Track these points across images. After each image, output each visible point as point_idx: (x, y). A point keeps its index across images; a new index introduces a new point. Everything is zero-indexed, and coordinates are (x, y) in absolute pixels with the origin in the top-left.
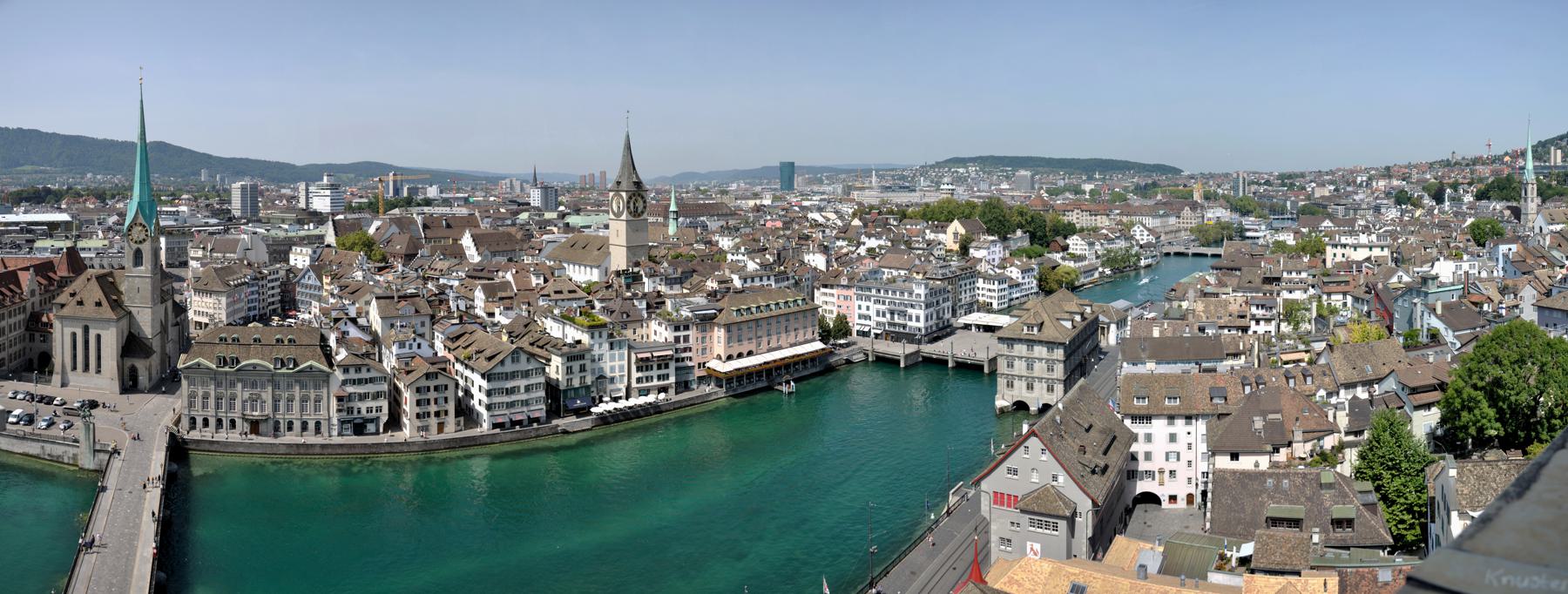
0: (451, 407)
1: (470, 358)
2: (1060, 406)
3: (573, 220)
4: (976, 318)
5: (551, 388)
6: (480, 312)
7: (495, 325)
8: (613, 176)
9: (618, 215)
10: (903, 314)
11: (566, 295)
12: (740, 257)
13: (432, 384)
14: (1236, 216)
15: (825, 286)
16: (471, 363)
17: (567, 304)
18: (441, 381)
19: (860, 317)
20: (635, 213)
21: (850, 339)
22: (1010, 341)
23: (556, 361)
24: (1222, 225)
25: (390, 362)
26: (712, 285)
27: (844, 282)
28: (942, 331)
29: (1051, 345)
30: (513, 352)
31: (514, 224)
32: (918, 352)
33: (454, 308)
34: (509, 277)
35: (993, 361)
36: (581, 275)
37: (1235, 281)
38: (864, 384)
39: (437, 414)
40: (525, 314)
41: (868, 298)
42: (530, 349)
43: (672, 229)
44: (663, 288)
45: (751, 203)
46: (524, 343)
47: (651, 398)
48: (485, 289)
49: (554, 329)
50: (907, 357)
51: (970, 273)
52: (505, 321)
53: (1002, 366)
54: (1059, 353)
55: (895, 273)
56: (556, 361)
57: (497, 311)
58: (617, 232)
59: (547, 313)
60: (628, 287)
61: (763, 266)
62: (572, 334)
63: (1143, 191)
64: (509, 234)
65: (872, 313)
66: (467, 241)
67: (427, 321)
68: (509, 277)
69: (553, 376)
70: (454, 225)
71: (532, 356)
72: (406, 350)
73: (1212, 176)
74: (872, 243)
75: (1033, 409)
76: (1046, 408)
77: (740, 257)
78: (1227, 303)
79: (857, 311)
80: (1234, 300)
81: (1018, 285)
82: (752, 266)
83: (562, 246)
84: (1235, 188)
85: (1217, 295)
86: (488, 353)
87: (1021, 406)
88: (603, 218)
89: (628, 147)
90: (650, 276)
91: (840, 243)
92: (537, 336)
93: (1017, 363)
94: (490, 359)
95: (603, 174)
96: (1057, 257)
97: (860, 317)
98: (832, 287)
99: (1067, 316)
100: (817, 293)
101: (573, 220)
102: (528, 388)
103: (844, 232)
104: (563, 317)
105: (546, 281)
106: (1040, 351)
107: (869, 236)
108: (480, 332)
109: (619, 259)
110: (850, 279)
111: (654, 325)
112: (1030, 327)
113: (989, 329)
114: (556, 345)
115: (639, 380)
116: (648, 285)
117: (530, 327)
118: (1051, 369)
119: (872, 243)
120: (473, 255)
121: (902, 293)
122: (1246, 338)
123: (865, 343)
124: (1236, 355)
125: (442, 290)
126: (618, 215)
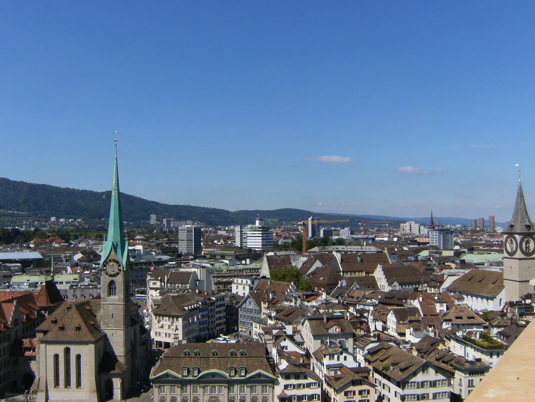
1: (386, 368)
7: (407, 343)
11: (465, 321)
13: (357, 388)
16: (388, 373)
40: (432, 335)
42: (436, 363)
46: (432, 358)
57: (408, 332)
59: (451, 336)
60: (521, 315)
68: (416, 304)
86: (403, 365)
88: (495, 257)
89: (521, 195)
94: (402, 370)
125: (361, 312)
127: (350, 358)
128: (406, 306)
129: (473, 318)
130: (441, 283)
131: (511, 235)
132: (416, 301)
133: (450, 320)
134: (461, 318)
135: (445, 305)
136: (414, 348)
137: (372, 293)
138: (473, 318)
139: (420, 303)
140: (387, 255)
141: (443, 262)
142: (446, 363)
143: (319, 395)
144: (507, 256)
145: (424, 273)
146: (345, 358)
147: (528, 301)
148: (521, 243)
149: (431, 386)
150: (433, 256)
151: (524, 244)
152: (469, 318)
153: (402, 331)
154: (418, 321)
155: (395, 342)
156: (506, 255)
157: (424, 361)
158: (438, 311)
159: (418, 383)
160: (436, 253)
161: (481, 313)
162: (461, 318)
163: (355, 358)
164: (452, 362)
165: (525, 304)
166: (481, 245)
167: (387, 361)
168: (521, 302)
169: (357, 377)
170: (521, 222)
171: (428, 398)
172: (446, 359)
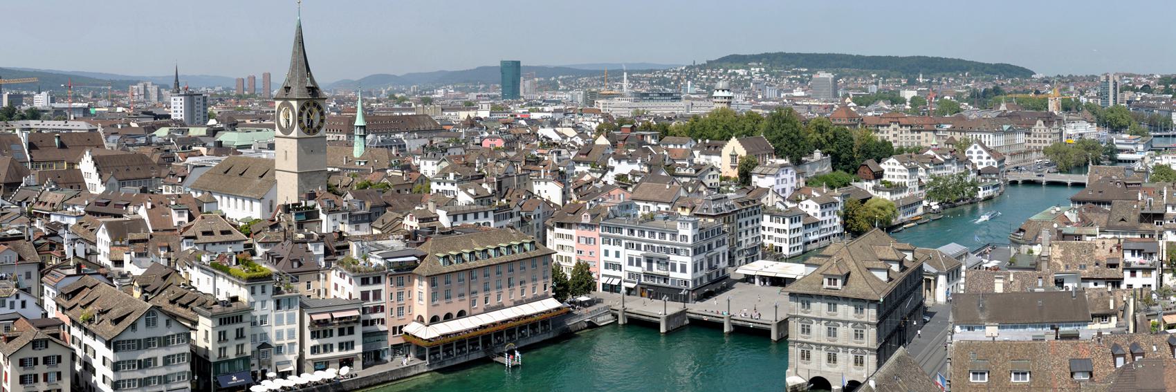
1: (90, 321)
2: (872, 383)
3: (227, 138)
6: (103, 259)
7: (124, 276)
8: (280, 77)
10: (664, 262)
11: (218, 237)
12: (449, 187)
14: (1104, 133)
15: (561, 225)
16: (92, 327)
17: (219, 249)
18: (52, 350)
19: (607, 266)
20: (309, 128)
21: (593, 295)
22: (805, 298)
23: (205, 324)
24: (1086, 145)
26: (411, 223)
28: (715, 285)
29: (860, 303)
31: (149, 143)
32: (683, 312)
33: (69, 255)
34: (142, 213)
35: (783, 325)
37: (1103, 219)
38: (613, 355)
40: (163, 262)
41: (618, 241)
43: (358, 150)
44: (346, 228)
46: (163, 300)
47: (330, 373)
48: (111, 228)
49: (202, 282)
51: (753, 208)
52: (137, 271)
54: (871, 314)
55: (653, 208)
56: (205, 324)
57: (127, 258)
58: (286, 154)
59: (193, 261)
61: (479, 198)
62: (226, 288)
63: (982, 99)
65: (623, 260)
66: (86, 166)
68: (142, 213)
69: (201, 343)
70: (69, 145)
71: (173, 317)
73: (1073, 79)
77: (449, 187)
78: (1092, 248)
79: (603, 258)
80: (1103, 243)
81: (816, 224)
82: (464, 199)
83: (213, 172)
84: (1103, 95)
85: (1079, 237)
86: (115, 314)
88: (266, 136)
90: (329, 212)
92: (179, 291)
93: (814, 327)
94: (117, 321)
95: (267, 77)
96: (868, 186)
97: (607, 266)
98: (570, 226)
99: (880, 265)
101: (227, 138)
102: (167, 361)
105: (191, 218)
107: (619, 159)
108: (104, 286)
109: (288, 190)
110: (594, 216)
111: (334, 277)
112: (833, 279)
113: (777, 282)
114: (205, 304)
115: (314, 350)
116: (327, 224)
117: (170, 280)
118: (859, 335)
119: (623, 168)
120: (95, 184)
121: (663, 234)
122: (1118, 294)
123: (613, 301)
124: (1104, 317)
125: (54, 230)
126: (286, 131)
128: (127, 218)
129: (229, 232)
131: (286, 100)
132: (143, 208)
133: (195, 238)
134: (211, 233)
135: (186, 215)
138: (229, 232)
139: (148, 210)
140: (103, 136)
142: (186, 306)
145: (159, 164)
147: (310, 203)
148: (300, 114)
149: (160, 346)
150: (174, 137)
152: (223, 233)
153: (119, 258)
155: (105, 275)
156: (278, 132)
157: (149, 305)
159: (139, 341)
160: (178, 131)
161: (241, 224)
162: (211, 233)
164: (193, 305)
165: (306, 207)
166: (248, 117)
167: (90, 308)
168: (299, 204)
169: (42, 335)
170: (301, 82)
171: (155, 364)
172: (184, 301)
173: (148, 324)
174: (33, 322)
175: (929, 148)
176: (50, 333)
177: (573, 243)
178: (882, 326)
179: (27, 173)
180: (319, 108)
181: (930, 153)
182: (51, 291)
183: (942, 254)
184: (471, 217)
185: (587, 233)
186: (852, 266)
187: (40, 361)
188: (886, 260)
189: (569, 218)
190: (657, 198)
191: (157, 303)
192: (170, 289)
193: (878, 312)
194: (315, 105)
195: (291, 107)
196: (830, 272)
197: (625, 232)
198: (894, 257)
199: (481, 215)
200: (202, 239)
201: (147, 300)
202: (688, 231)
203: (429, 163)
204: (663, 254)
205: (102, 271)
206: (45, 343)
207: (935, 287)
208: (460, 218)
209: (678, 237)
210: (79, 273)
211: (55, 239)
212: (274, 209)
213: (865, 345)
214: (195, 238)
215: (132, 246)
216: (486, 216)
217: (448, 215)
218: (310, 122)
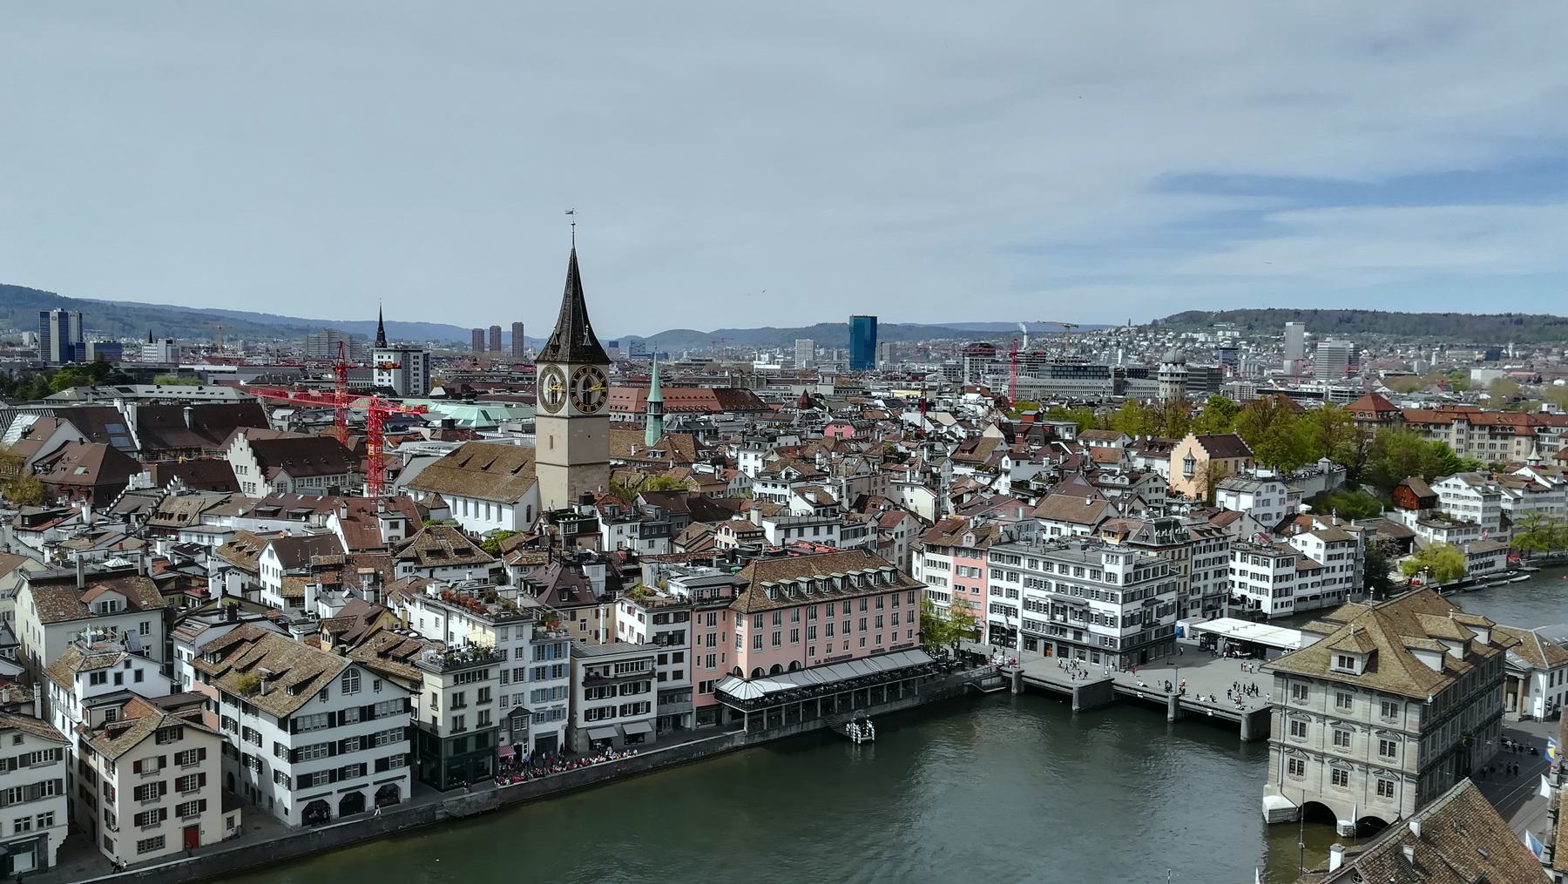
0: (212, 792)
2: (1414, 827)
4: (1225, 626)
5: (422, 738)
9: (554, 405)
12: (779, 491)
13: (170, 750)
15: (933, 549)
16: (255, 700)
17: (452, 575)
18: (191, 741)
20: (587, 408)
22: (1300, 682)
25: (70, 711)
26: (726, 539)
27: (969, 541)
29: (1391, 700)
30: (346, 674)
32: (1108, 684)
33: (214, 588)
34: (333, 524)
35: (1261, 720)
36: (480, 519)
39: (180, 811)
41: (1013, 576)
43: (650, 437)
44: (638, 546)
45: (798, 390)
46: (368, 653)
49: (426, 621)
50: (1083, 690)
52: (326, 611)
53: (1280, 730)
54: (1410, 720)
55: (1066, 531)
56: (434, 684)
57: (308, 594)
58: (551, 440)
61: (823, 506)
62: (467, 632)
64: (331, 440)
66: (239, 454)
67: (156, 621)
68: (333, 524)
69: (425, 716)
71: (384, 675)
72: (110, 687)
74: (1026, 471)
75: (1345, 822)
76: (1370, 828)
77: (779, 491)
81: (1317, 571)
82: (799, 506)
83: (440, 467)
86: (293, 678)
87: (1317, 816)
90: (612, 520)
91: (959, 470)
92: (392, 637)
93: (1313, 727)
94: (298, 688)
95: (518, 328)
96: (1410, 518)
98: (945, 550)
100: (917, 563)
103: (969, 449)
104: (447, 598)
105: (410, 531)
106: (1361, 708)
109: (554, 490)
110: (981, 540)
111: (621, 614)
113: (1255, 650)
118: (1387, 748)
121: (1079, 571)
126: (554, 405)
127: (152, 671)
129: (468, 552)
130: (396, 473)
136: (325, 631)
137: (222, 503)
138: (468, 552)
139: (341, 521)
141: (401, 426)
142: (404, 660)
143: (59, 782)
144: (545, 412)
146: (139, 676)
147: (586, 510)
148: (573, 384)
151: (580, 387)
153: (296, 593)
154: (338, 567)
155: (275, 621)
156: (540, 409)
157: (348, 661)
158: (385, 540)
163: (168, 671)
166: (490, 385)
169: (171, 721)
173: (345, 689)
174: (154, 702)
175: (1523, 465)
176: (182, 715)
177: (949, 575)
178: (1428, 740)
179: (137, 469)
180: (600, 376)
181: (1527, 472)
182: (185, 651)
183: (1541, 639)
184: (808, 532)
185: (969, 561)
186: (1380, 640)
187: (170, 760)
188: (1439, 638)
189: (945, 540)
190: (1074, 518)
191: (360, 658)
192: (380, 636)
193: (1423, 718)
194: (594, 371)
195: (561, 375)
196: (1342, 646)
197: (1024, 564)
198: (1455, 633)
199: (824, 530)
200: (427, 561)
201: (343, 653)
202: (1118, 569)
203: (751, 456)
204: (1079, 598)
205: (270, 614)
206: (177, 732)
207: (1526, 692)
208: (794, 532)
209: (1103, 576)
210: (233, 618)
211: (190, 570)
212: (533, 517)
213: (1398, 766)
214: (416, 560)
215: (318, 577)
216: (830, 532)
217: (778, 527)
218: (587, 396)
